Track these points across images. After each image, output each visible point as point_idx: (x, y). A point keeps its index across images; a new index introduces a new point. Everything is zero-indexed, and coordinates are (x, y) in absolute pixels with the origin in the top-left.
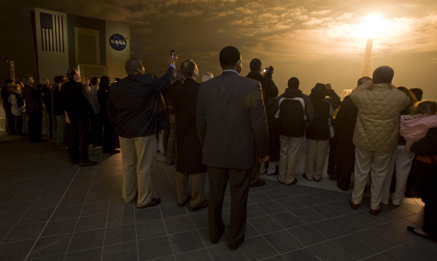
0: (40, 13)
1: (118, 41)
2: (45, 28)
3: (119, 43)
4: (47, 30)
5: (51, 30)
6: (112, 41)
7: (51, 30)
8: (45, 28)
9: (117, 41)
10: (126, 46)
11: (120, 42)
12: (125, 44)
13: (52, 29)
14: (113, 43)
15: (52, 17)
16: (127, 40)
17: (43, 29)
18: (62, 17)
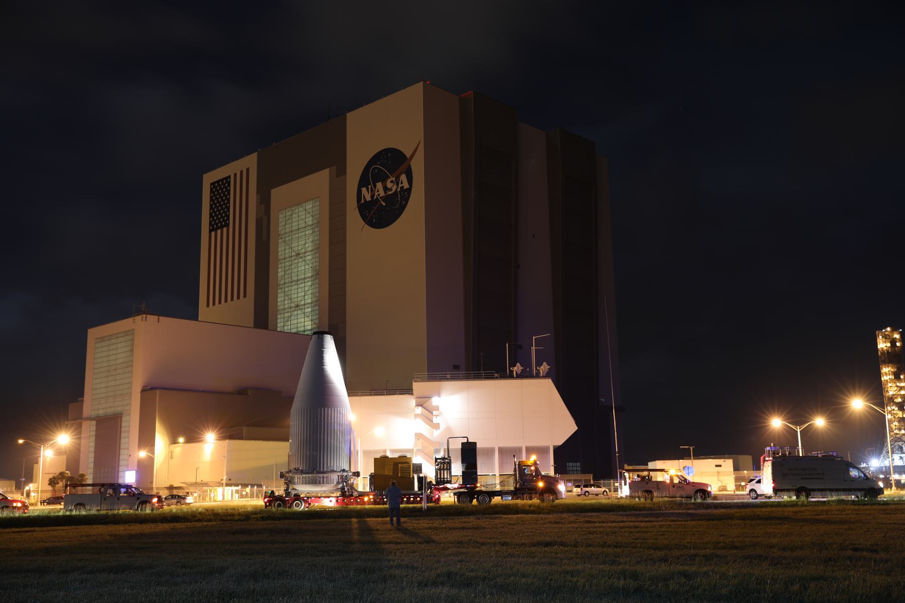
0: (211, 184)
1: (384, 181)
2: (215, 230)
3: (386, 189)
4: (219, 231)
5: (225, 229)
6: (364, 190)
7: (225, 229)
8: (218, 228)
9: (379, 185)
10: (409, 190)
11: (389, 185)
12: (406, 186)
13: (227, 225)
14: (368, 198)
15: (229, 183)
16: (412, 163)
17: (213, 233)
18: (248, 170)
